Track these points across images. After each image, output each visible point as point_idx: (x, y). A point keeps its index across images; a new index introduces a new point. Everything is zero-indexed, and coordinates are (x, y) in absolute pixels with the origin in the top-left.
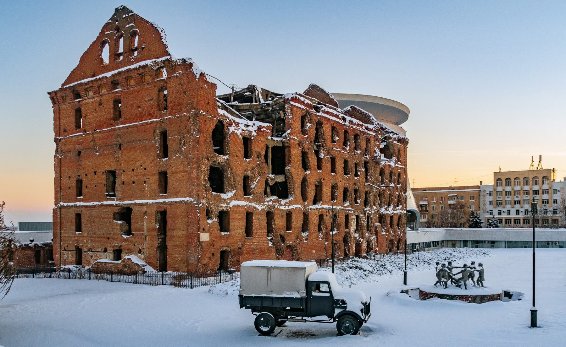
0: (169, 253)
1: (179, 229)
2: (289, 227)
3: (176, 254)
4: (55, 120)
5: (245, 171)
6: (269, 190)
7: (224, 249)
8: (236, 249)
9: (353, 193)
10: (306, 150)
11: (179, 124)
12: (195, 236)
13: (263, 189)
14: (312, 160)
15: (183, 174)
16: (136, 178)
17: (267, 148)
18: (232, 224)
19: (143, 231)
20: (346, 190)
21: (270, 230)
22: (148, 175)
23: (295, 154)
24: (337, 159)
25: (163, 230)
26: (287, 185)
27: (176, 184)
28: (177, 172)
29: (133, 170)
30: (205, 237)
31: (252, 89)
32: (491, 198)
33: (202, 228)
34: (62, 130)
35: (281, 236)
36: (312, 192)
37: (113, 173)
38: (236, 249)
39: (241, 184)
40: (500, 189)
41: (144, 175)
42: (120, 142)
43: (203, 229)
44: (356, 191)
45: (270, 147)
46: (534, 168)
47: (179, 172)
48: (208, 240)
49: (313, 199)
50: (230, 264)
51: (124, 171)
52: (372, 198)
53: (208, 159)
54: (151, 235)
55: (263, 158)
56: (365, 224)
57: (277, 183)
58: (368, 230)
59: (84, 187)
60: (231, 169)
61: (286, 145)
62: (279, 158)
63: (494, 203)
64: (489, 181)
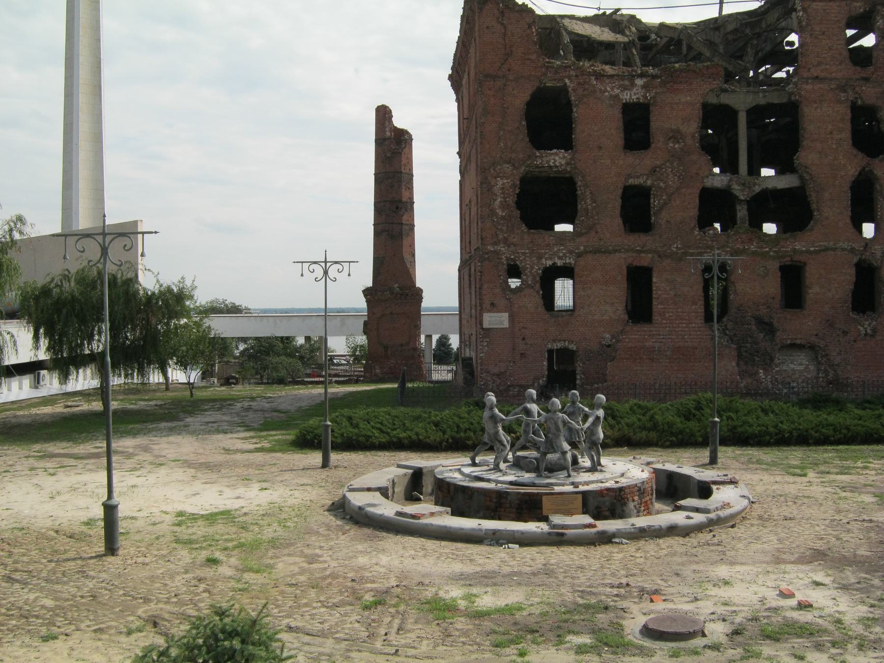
5: (630, 176)
35: (760, 321)
43: (493, 304)
60: (583, 177)
61: (793, 98)
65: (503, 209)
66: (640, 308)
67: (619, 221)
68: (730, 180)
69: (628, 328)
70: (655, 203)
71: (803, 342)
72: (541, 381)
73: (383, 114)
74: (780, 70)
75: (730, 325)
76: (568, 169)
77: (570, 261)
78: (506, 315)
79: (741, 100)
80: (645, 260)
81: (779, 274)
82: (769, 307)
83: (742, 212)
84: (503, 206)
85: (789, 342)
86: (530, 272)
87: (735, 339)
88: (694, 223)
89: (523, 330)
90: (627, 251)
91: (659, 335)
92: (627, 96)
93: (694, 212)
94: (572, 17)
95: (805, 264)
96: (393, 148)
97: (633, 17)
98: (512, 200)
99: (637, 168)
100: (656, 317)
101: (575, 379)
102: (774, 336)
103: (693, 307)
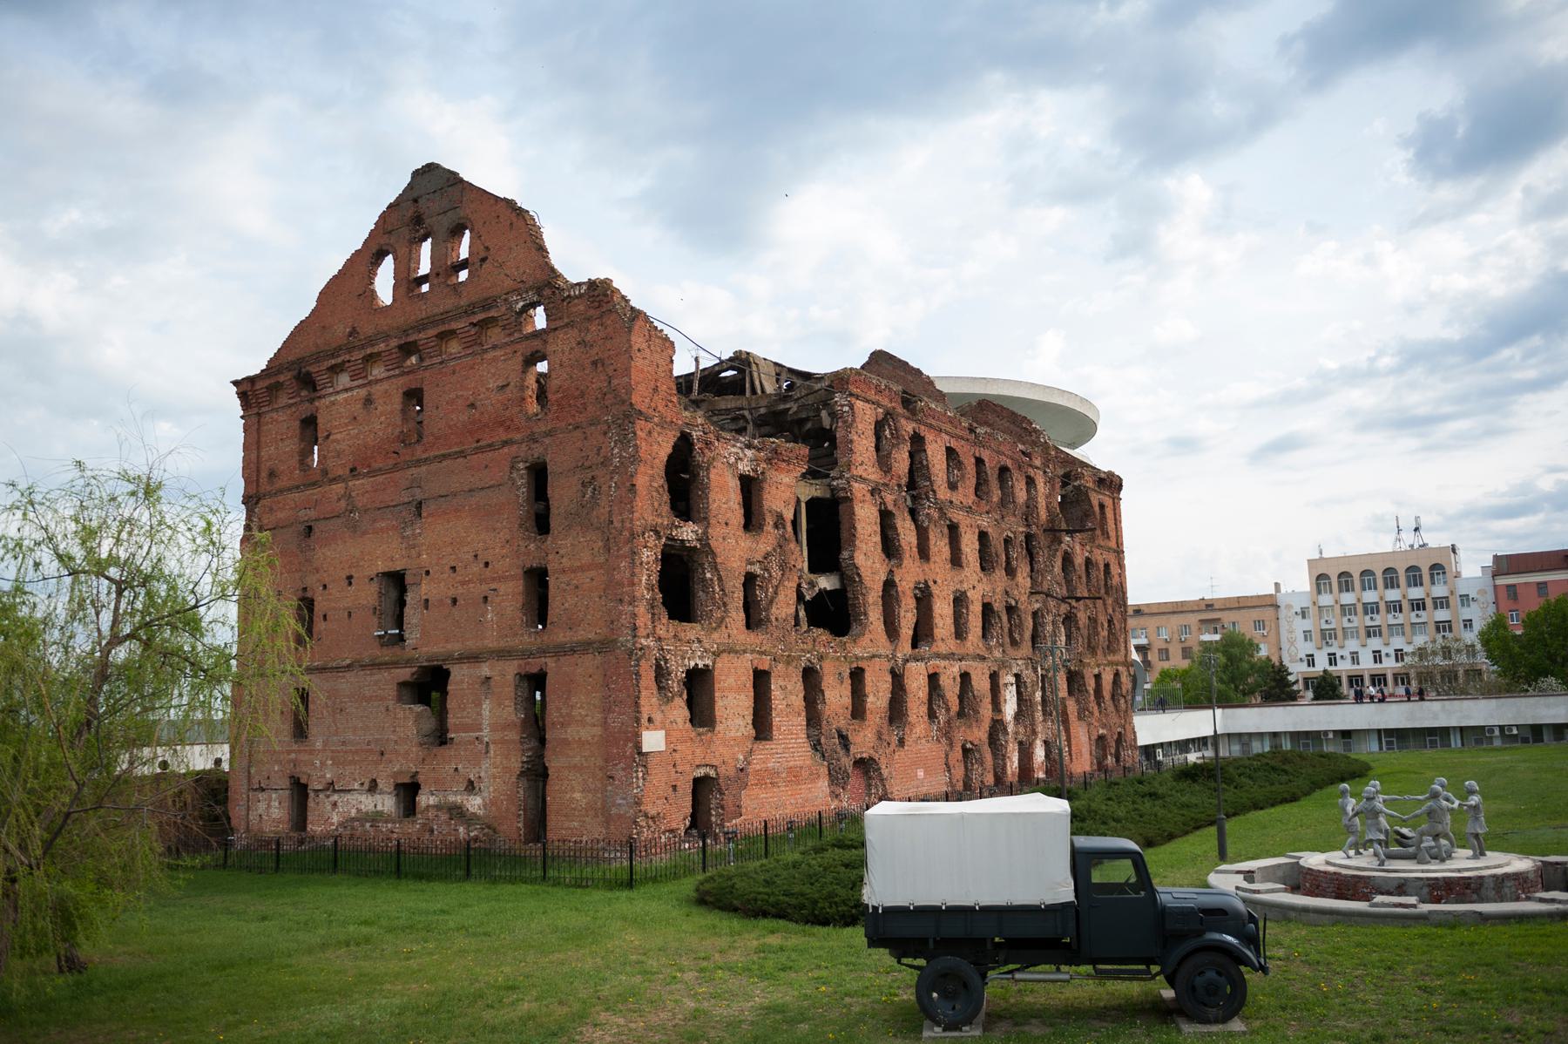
0: (553, 787)
1: (582, 723)
2: (858, 710)
3: (573, 790)
4: (246, 447)
6: (802, 614)
7: (700, 772)
8: (732, 772)
9: (1005, 618)
10: (890, 507)
11: (579, 444)
12: (628, 740)
13: (792, 610)
14: (906, 533)
15: (593, 573)
16: (460, 590)
17: (798, 501)
18: (719, 704)
19: (481, 730)
20: (987, 609)
21: (813, 718)
22: (494, 579)
23: (865, 517)
24: (962, 529)
25: (536, 727)
26: (846, 598)
27: (571, 601)
28: (574, 570)
29: (453, 568)
30: (653, 741)
31: (742, 361)
32: (1307, 624)
33: (645, 717)
34: (264, 474)
36: (909, 615)
37: (397, 581)
38: (732, 772)
39: (739, 595)
40: (1326, 599)
41: (481, 581)
42: (419, 497)
43: (650, 720)
44: (1010, 610)
45: (804, 499)
46: (1405, 547)
47: (582, 569)
48: (663, 748)
49: (911, 632)
51: (428, 573)
52: (1049, 628)
53: (657, 533)
54: (503, 742)
55: (789, 529)
56: (1038, 695)
57: (823, 593)
58: (1044, 711)
59: (318, 618)
61: (842, 494)
62: (826, 529)
63: (1316, 636)
64: (1299, 583)
75: (823, 740)
98: (655, 579)
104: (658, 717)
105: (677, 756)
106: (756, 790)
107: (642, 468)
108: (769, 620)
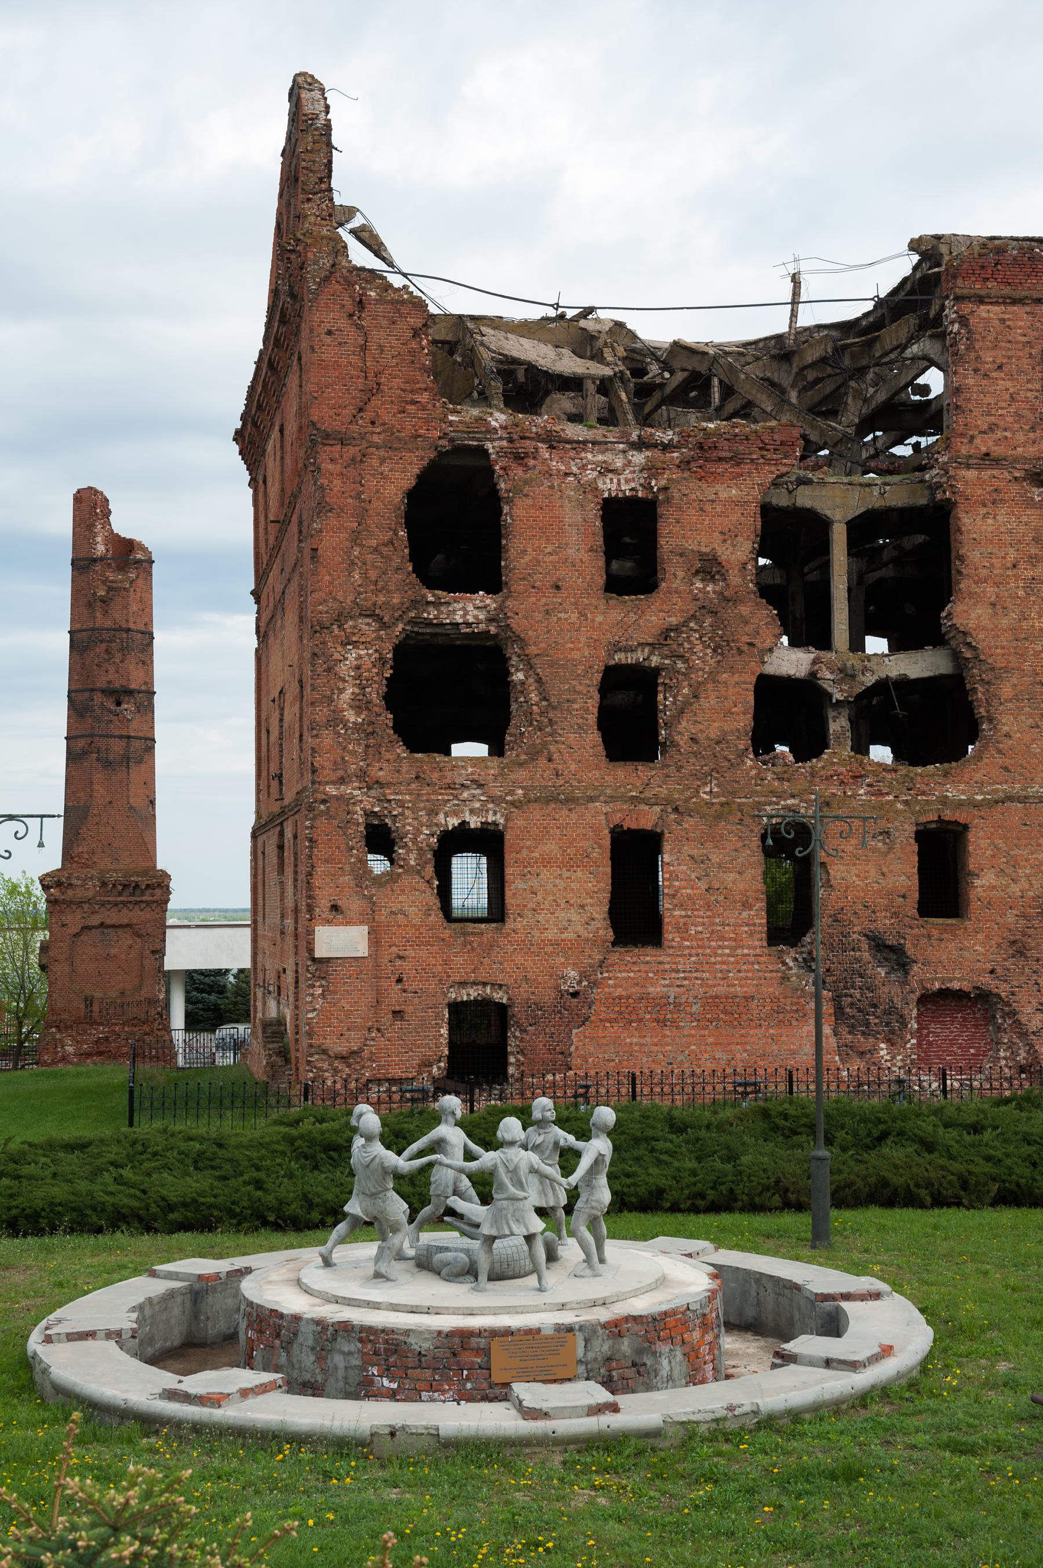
8: (548, 997)
33: (323, 904)
38: (548, 997)
43: (335, 908)
48: (362, 950)
50: (519, 1064)
61: (939, 496)
65: (358, 710)
66: (636, 914)
67: (594, 737)
68: (814, 662)
69: (614, 958)
70: (665, 700)
71: (966, 986)
72: (435, 1070)
73: (90, 507)
74: (900, 442)
75: (820, 953)
76: (493, 630)
77: (495, 817)
78: (365, 929)
79: (838, 499)
80: (647, 819)
81: (916, 848)
82: (895, 915)
83: (838, 725)
84: (360, 704)
85: (937, 985)
86: (414, 841)
87: (828, 979)
88: (745, 743)
89: (398, 962)
90: (612, 799)
91: (678, 971)
92: (609, 486)
93: (744, 721)
94: (496, 323)
95: (966, 827)
96: (109, 583)
97: (620, 325)
98: (375, 694)
99: (630, 628)
100: (670, 935)
101: (505, 1064)
102: (907, 973)
103: (745, 914)
104: (354, 905)
105: (406, 965)
106: (612, 1030)
107: (332, 521)
108: (675, 744)
